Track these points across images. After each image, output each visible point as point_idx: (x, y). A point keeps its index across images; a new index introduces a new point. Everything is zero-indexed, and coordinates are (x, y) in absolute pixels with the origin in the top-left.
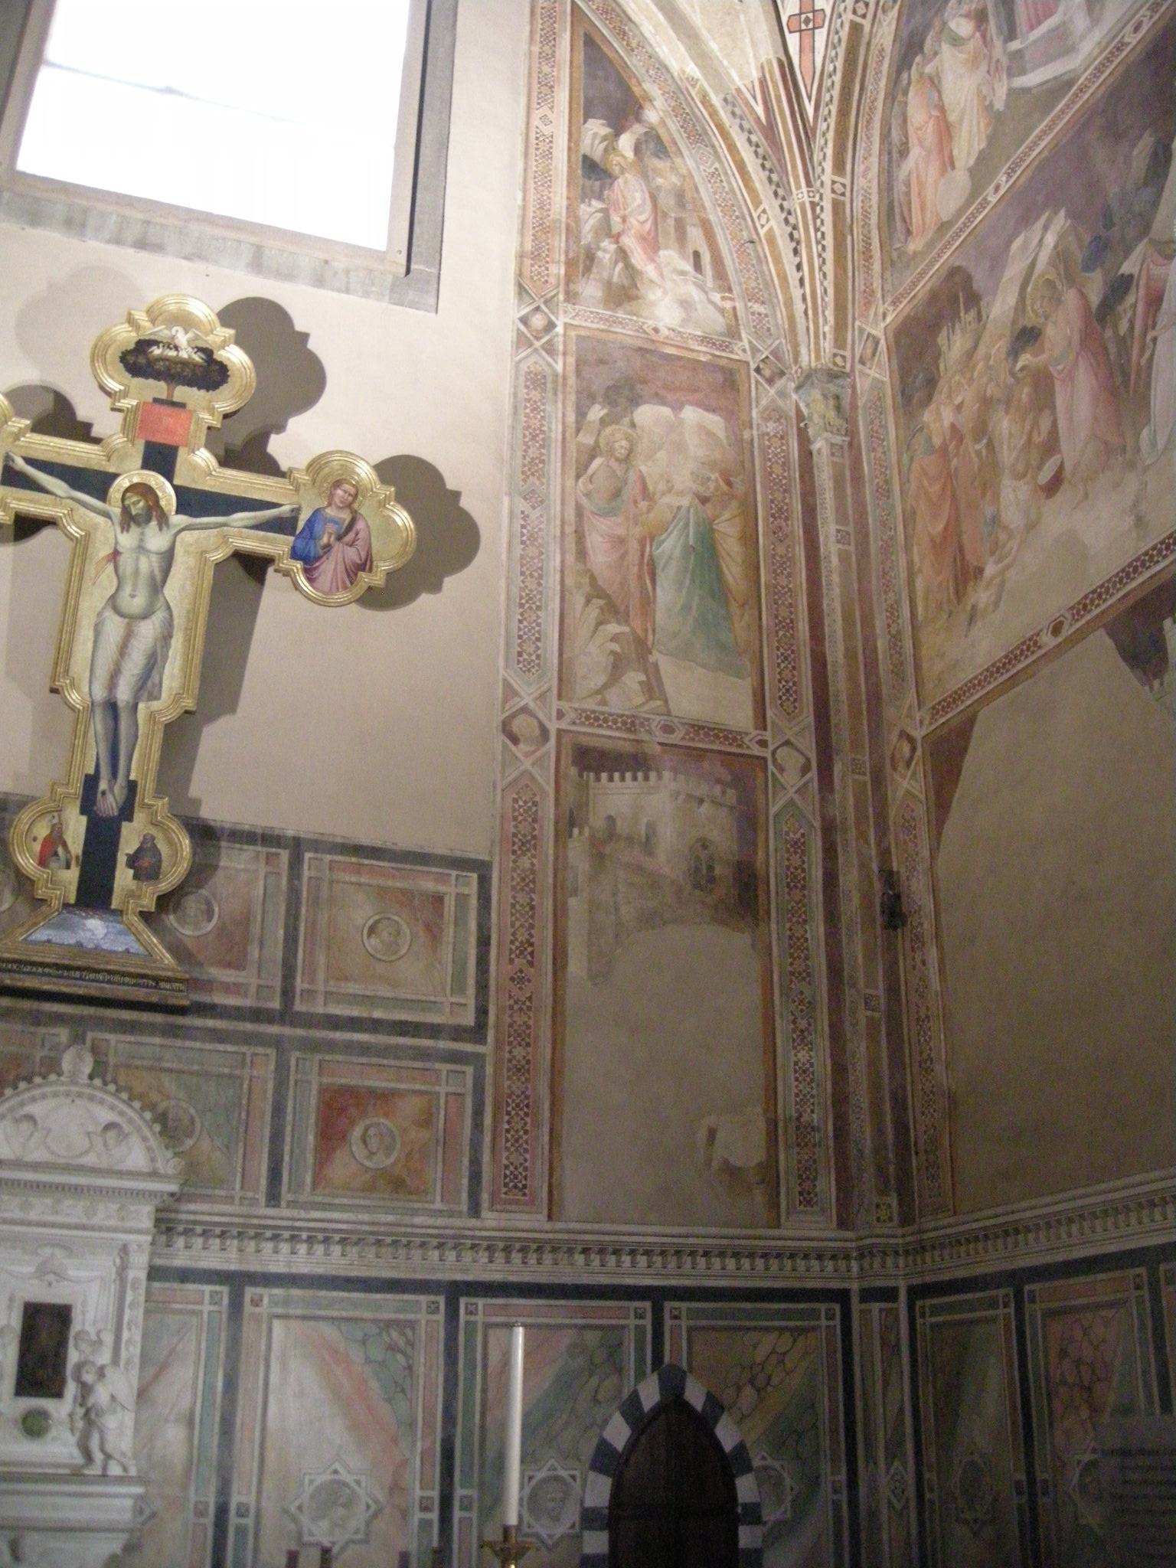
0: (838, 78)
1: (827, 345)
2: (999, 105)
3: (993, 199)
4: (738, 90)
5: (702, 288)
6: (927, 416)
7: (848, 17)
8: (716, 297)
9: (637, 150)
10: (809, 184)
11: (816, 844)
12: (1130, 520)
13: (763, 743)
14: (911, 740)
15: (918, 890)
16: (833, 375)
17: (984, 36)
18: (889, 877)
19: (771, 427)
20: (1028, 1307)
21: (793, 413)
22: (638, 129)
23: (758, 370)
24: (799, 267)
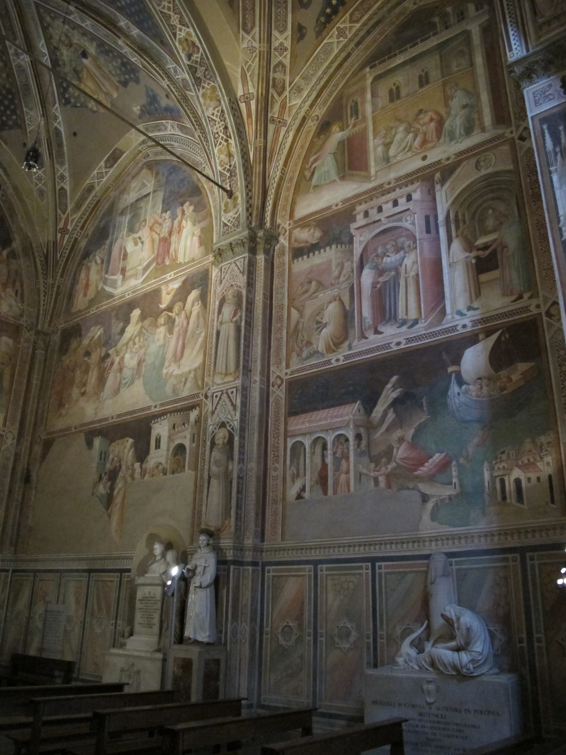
0: (68, 252)
1: (46, 326)
2: (99, 288)
3: (92, 313)
4: (41, 244)
5: (16, 301)
6: (64, 358)
7: (75, 236)
8: (19, 305)
9: (8, 256)
10: (53, 278)
11: (12, 458)
12: (94, 412)
13: (4, 431)
14: (41, 439)
15: (34, 475)
16: (46, 334)
17: (102, 267)
18: (28, 471)
19: (26, 345)
20: (36, 578)
21: (32, 341)
22: (9, 249)
23: (26, 327)
24: (44, 300)
